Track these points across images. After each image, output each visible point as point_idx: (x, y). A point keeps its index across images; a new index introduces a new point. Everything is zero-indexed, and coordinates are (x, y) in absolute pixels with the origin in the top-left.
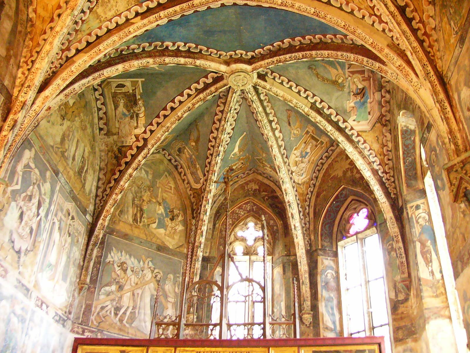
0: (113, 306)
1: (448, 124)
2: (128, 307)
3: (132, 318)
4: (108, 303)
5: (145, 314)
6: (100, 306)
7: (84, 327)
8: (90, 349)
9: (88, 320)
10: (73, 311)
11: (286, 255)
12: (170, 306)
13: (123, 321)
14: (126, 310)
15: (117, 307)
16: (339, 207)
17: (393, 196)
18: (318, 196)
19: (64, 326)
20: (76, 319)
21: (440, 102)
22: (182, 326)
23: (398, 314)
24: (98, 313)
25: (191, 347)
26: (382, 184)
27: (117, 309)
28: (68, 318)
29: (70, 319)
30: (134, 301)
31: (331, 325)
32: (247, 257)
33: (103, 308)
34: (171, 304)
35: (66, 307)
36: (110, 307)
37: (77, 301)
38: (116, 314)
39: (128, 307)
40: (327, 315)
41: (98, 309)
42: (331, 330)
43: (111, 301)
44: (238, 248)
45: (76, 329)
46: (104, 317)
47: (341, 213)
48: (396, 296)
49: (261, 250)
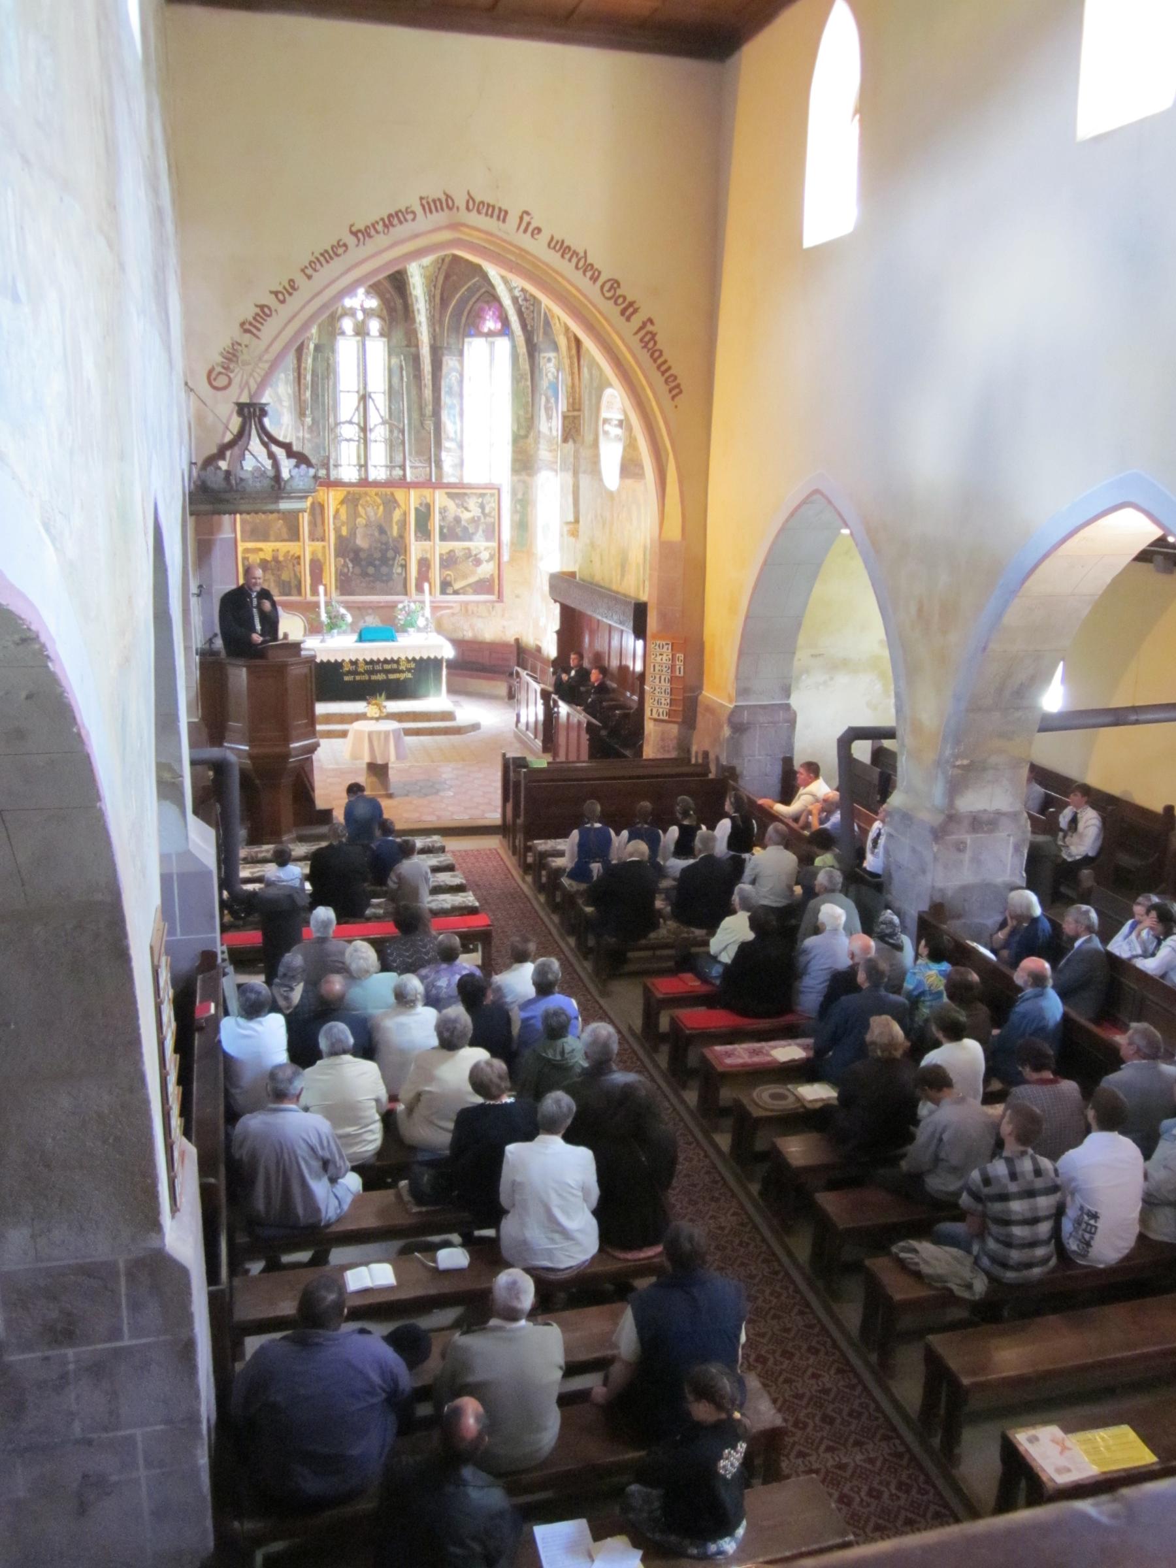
1: (573, 379)
11: (408, 346)
12: (285, 411)
16: (469, 298)
17: (529, 328)
18: (447, 277)
21: (570, 358)
22: (331, 467)
26: (520, 314)
31: (452, 435)
32: (359, 338)
42: (452, 440)
44: (347, 324)
47: (471, 303)
48: (518, 429)
49: (374, 326)
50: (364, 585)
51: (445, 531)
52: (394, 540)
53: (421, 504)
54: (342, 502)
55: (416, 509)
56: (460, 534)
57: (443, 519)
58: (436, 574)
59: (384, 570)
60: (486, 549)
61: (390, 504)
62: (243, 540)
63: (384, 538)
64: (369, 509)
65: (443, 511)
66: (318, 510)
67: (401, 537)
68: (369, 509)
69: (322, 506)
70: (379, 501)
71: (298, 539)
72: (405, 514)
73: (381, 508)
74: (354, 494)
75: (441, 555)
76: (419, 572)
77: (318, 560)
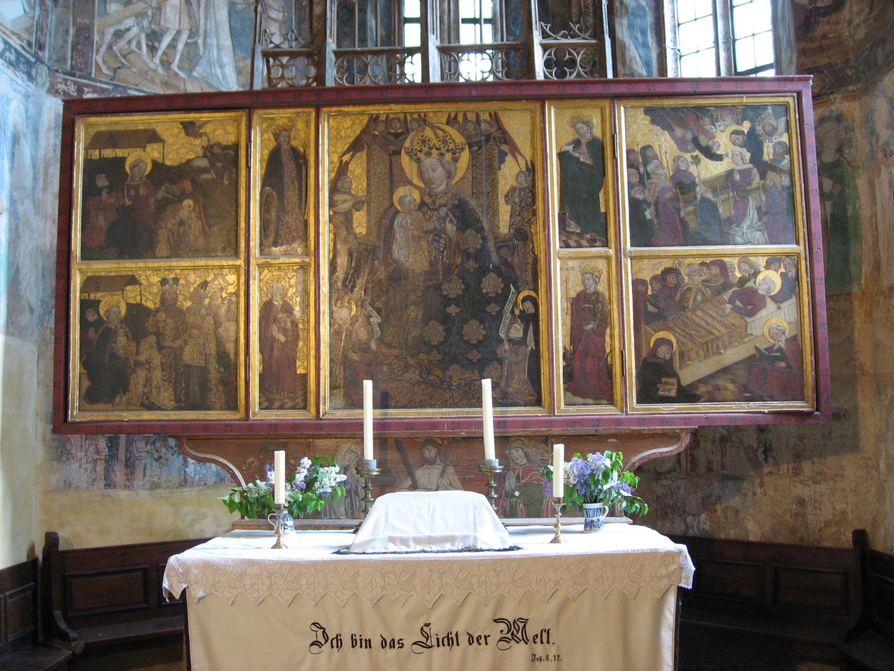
0: (142, 29)
2: (179, 32)
3: (192, 58)
4: (130, 22)
5: (219, 49)
6: (112, 30)
7: (80, 80)
8: (105, 124)
9: (87, 63)
10: (48, 41)
13: (170, 64)
14: (175, 40)
15: (154, 32)
19: (31, 78)
20: (58, 61)
23: (812, 40)
24: (110, 48)
25: (354, 105)
27: (154, 37)
28: (39, 60)
29: (42, 62)
30: (191, 17)
33: (118, 35)
34: (277, 25)
35: (28, 30)
36: (135, 30)
37: (53, 18)
38: (152, 49)
39: (179, 32)
40: (632, 47)
41: (108, 38)
43: (137, 16)
45: (61, 87)
46: (125, 57)
50: (413, 375)
51: (648, 214)
52: (502, 243)
53: (577, 143)
54: (355, 147)
55: (562, 155)
56: (692, 224)
57: (641, 179)
58: (624, 345)
59: (474, 331)
60: (773, 261)
61: (490, 144)
62: (88, 254)
63: (472, 241)
64: (430, 162)
65: (641, 159)
66: (288, 168)
67: (523, 234)
68: (430, 162)
69: (300, 160)
70: (459, 139)
71: (236, 255)
72: (531, 170)
73: (465, 156)
74: (388, 121)
75: (636, 282)
76: (575, 334)
77: (288, 309)
